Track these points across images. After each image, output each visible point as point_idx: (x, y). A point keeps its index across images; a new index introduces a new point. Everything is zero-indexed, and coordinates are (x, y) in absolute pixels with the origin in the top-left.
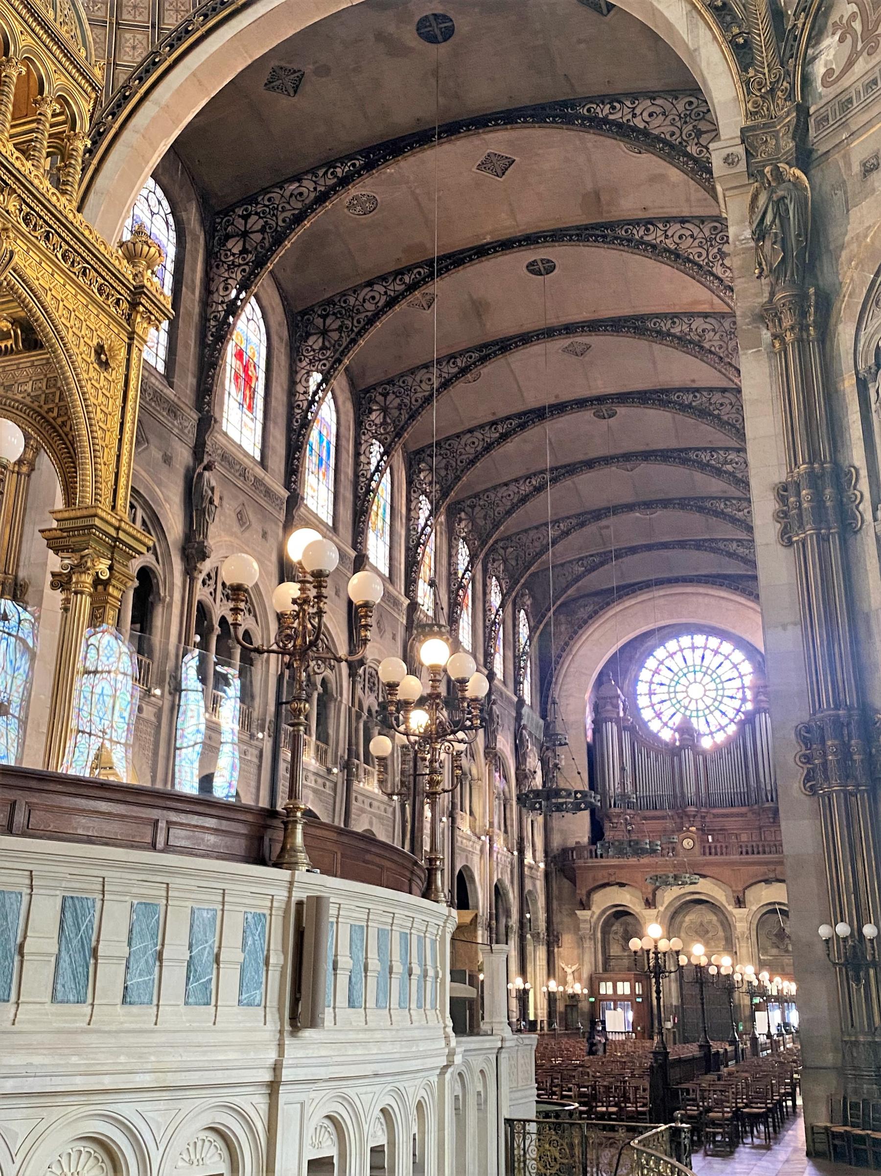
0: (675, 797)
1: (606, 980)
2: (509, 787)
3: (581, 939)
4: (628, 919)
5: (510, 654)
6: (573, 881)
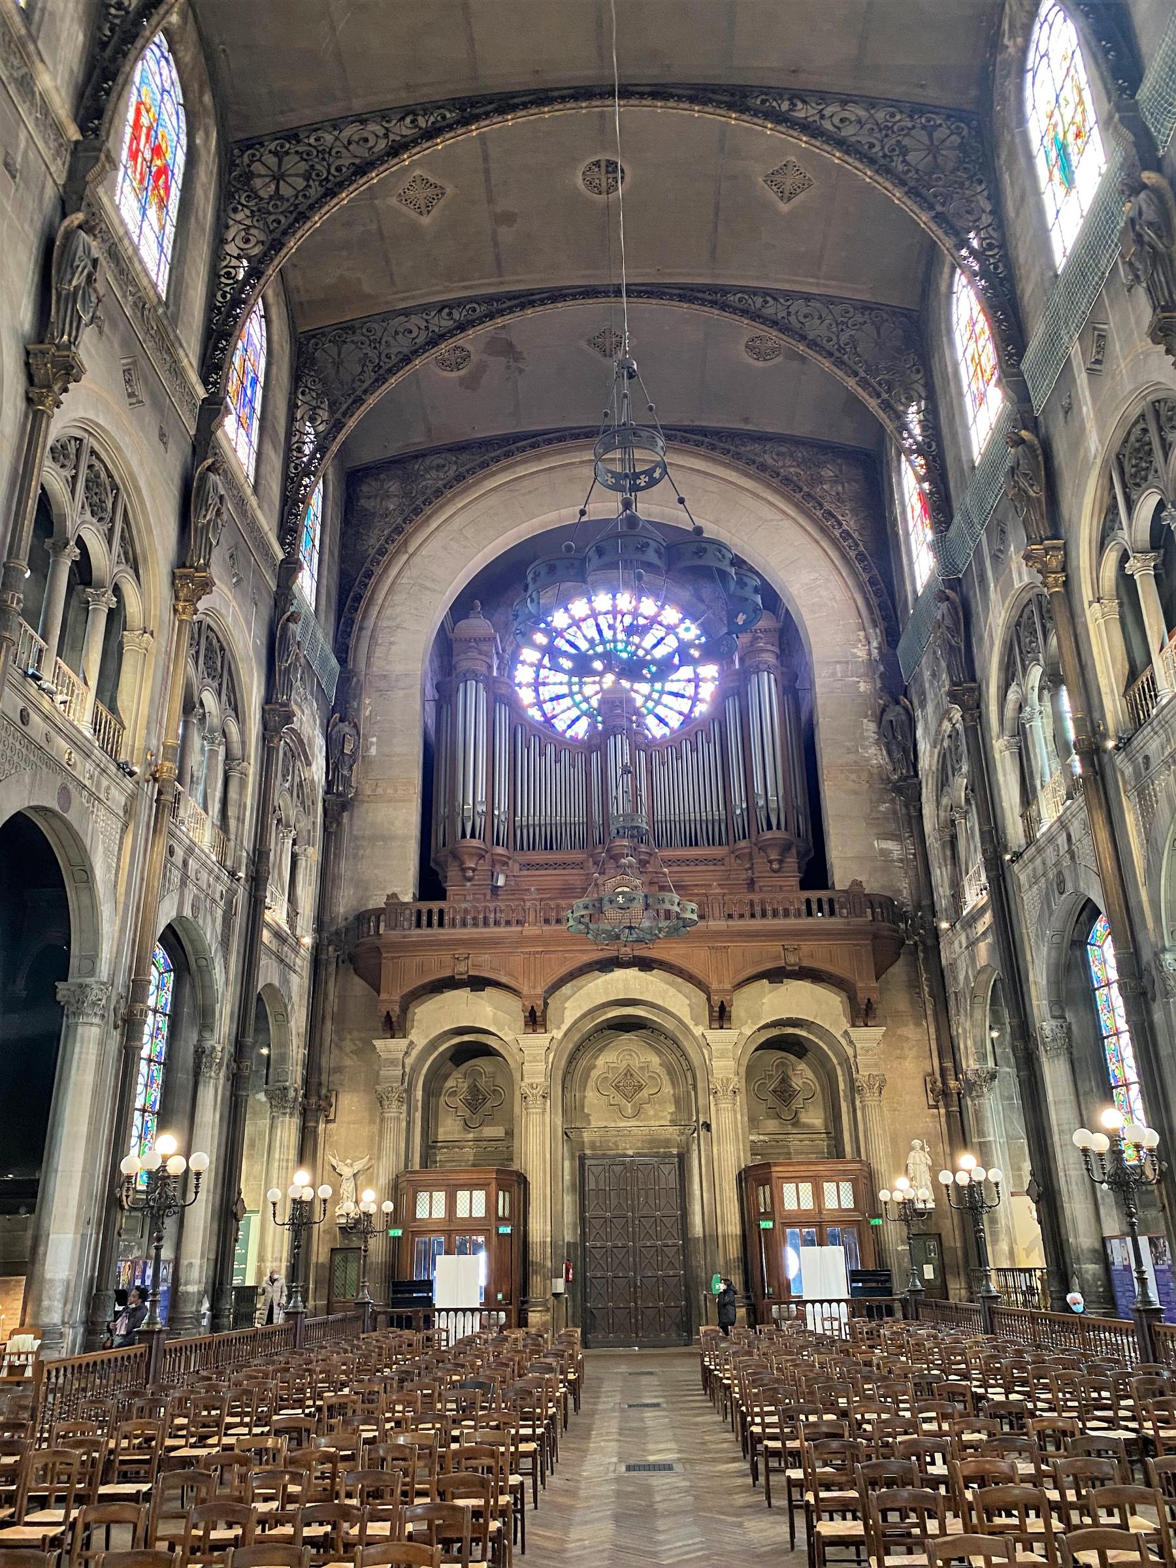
0: (589, 823)
1: (431, 1187)
2: (242, 733)
4: (482, 1063)
5: (275, 461)
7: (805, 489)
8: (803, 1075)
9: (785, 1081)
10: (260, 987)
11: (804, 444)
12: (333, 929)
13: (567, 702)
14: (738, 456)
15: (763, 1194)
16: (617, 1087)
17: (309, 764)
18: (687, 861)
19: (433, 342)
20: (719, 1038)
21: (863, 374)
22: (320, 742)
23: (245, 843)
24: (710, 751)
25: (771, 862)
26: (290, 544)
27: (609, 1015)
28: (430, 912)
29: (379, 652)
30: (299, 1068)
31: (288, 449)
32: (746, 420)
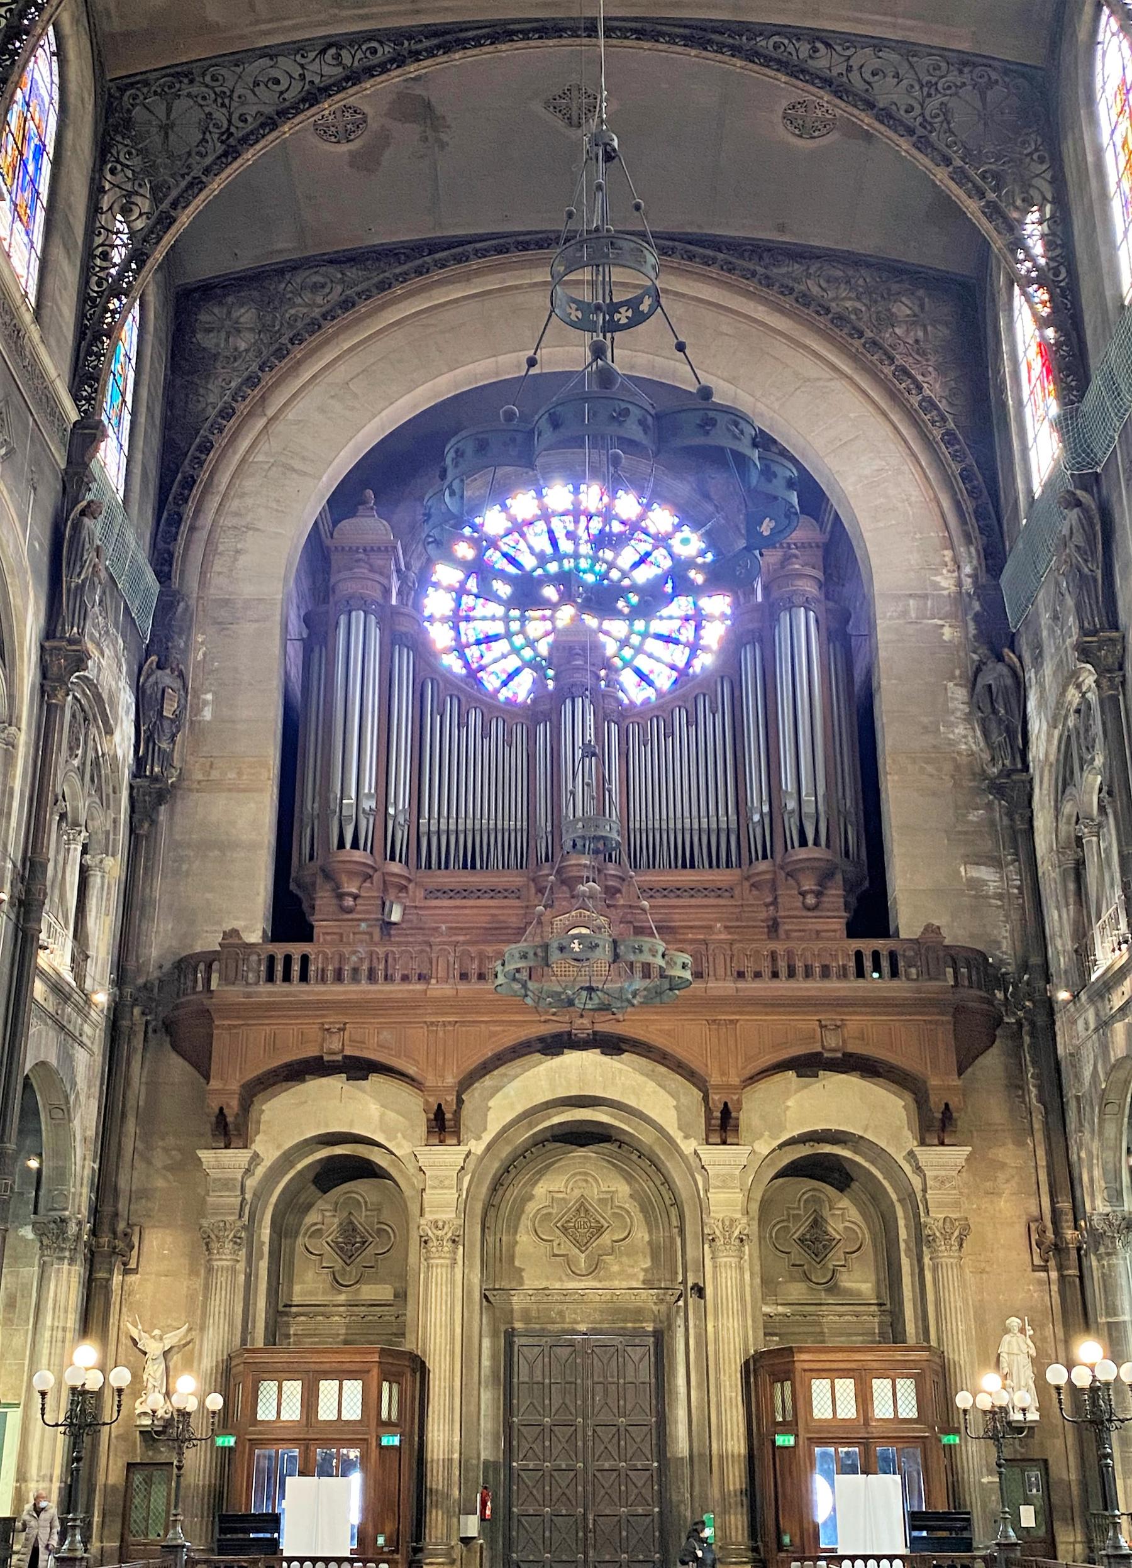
1: (280, 1374)
3: (207, 1242)
4: (361, 1188)
5: (68, 272)
6: (202, 1064)
7: (868, 334)
8: (844, 1215)
9: (817, 1223)
10: (28, 1066)
11: (869, 265)
12: (141, 981)
13: (502, 646)
14: (768, 282)
15: (782, 1394)
16: (565, 1230)
17: (110, 732)
18: (678, 891)
19: (312, 98)
20: (720, 1158)
21: (958, 162)
22: (126, 699)
23: (11, 849)
24: (715, 726)
25: (803, 894)
26: (88, 399)
27: (556, 1120)
28: (288, 959)
29: (219, 565)
30: (85, 1191)
31: (89, 254)
32: (782, 228)
